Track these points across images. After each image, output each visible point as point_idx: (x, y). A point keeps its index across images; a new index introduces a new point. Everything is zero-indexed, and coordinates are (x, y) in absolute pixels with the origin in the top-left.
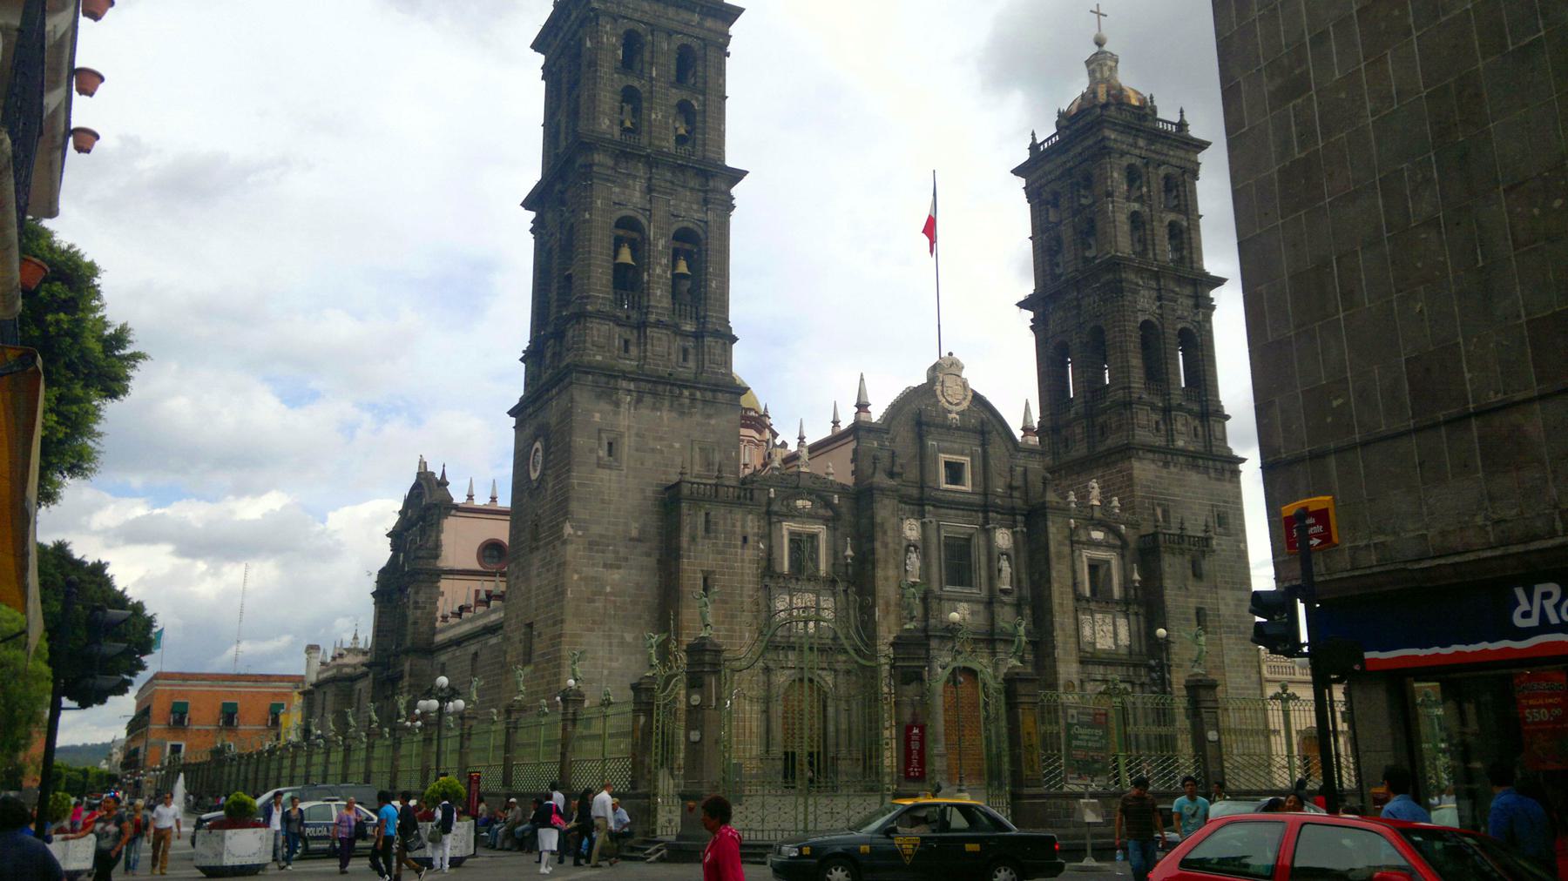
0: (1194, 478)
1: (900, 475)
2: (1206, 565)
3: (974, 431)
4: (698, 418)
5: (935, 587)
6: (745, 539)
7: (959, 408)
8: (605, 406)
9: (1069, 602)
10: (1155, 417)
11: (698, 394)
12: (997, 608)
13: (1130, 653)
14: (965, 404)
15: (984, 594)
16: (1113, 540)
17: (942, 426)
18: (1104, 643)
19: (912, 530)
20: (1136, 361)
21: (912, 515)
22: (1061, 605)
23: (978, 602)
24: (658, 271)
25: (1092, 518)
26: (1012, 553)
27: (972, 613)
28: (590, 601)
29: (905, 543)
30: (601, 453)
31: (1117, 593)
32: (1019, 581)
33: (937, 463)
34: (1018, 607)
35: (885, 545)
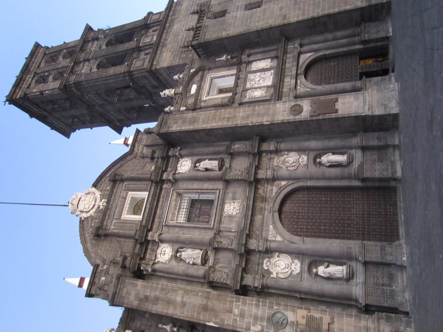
0: (176, 27)
1: (125, 258)
2: (216, 9)
3: (113, 187)
5: (208, 236)
7: (98, 200)
9: (226, 112)
12: (230, 176)
13: (277, 57)
14: (98, 193)
15: (220, 185)
16: (197, 78)
17: (105, 214)
18: (268, 79)
19: (164, 254)
20: (112, 71)
21: (154, 251)
22: (228, 119)
23: (225, 193)
25: (181, 94)
26: (196, 158)
27: (234, 199)
29: (174, 263)
32: (215, 153)
33: (126, 222)
34: (232, 155)
35: (157, 299)
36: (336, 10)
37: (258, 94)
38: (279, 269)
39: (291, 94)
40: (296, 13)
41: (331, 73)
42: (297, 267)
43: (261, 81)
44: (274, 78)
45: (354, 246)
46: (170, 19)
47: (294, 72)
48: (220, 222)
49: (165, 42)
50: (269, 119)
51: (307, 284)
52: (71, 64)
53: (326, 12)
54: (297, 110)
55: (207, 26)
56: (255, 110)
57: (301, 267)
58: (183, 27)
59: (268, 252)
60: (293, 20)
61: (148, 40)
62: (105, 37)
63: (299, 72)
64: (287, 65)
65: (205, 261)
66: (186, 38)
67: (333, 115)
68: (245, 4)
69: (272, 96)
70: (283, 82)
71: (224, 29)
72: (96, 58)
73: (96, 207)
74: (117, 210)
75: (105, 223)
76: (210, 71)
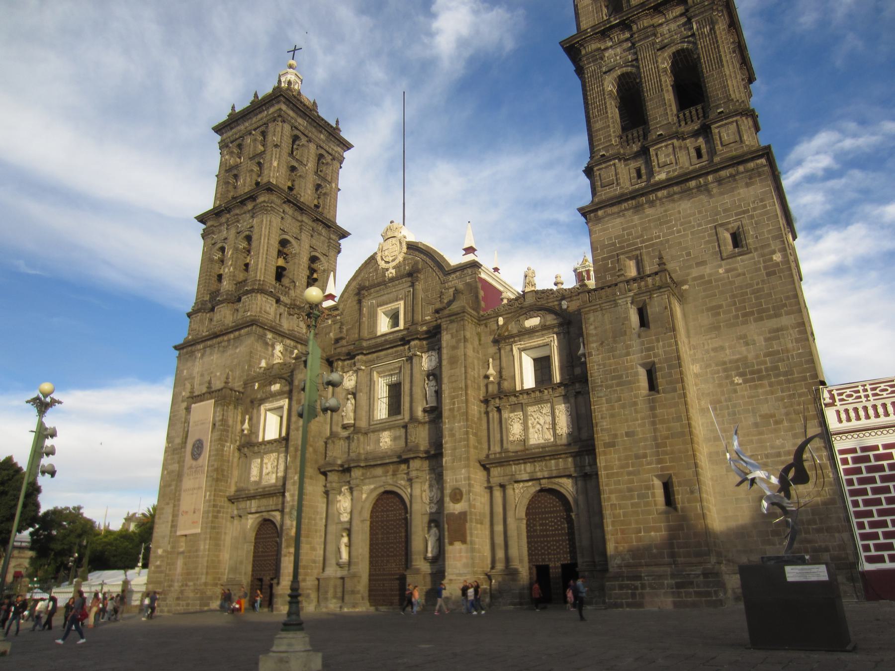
1: (342, 338)
4: (230, 352)
6: (214, 425)
7: (394, 264)
8: (189, 364)
10: (633, 165)
11: (232, 336)
14: (400, 258)
16: (551, 319)
17: (379, 284)
24: (226, 270)
27: (395, 439)
28: (170, 485)
30: (184, 394)
31: (557, 377)
33: (373, 317)
36: (609, 528)
37: (516, 429)
38: (342, 502)
39: (506, 478)
40: (617, 463)
41: (552, 526)
42: (345, 518)
43: (538, 426)
44: (538, 446)
45: (363, 569)
46: (710, 178)
47: (539, 475)
48: (373, 432)
49: (646, 206)
50: (449, 465)
51: (332, 528)
52: (616, 20)
53: (607, 512)
54: (457, 496)
55: (616, 305)
56: (460, 442)
57: (345, 522)
58: (681, 225)
59: (351, 490)
60: (601, 461)
61: (662, 159)
62: (693, 35)
63: (543, 481)
64: (553, 462)
65: (345, 427)
66: (653, 245)
67: (446, 541)
68: (656, 360)
69: (507, 451)
70: (525, 463)
71: (602, 344)
72: (637, 60)
73: (387, 266)
74: (384, 298)
75: (372, 290)
76: (562, 335)
